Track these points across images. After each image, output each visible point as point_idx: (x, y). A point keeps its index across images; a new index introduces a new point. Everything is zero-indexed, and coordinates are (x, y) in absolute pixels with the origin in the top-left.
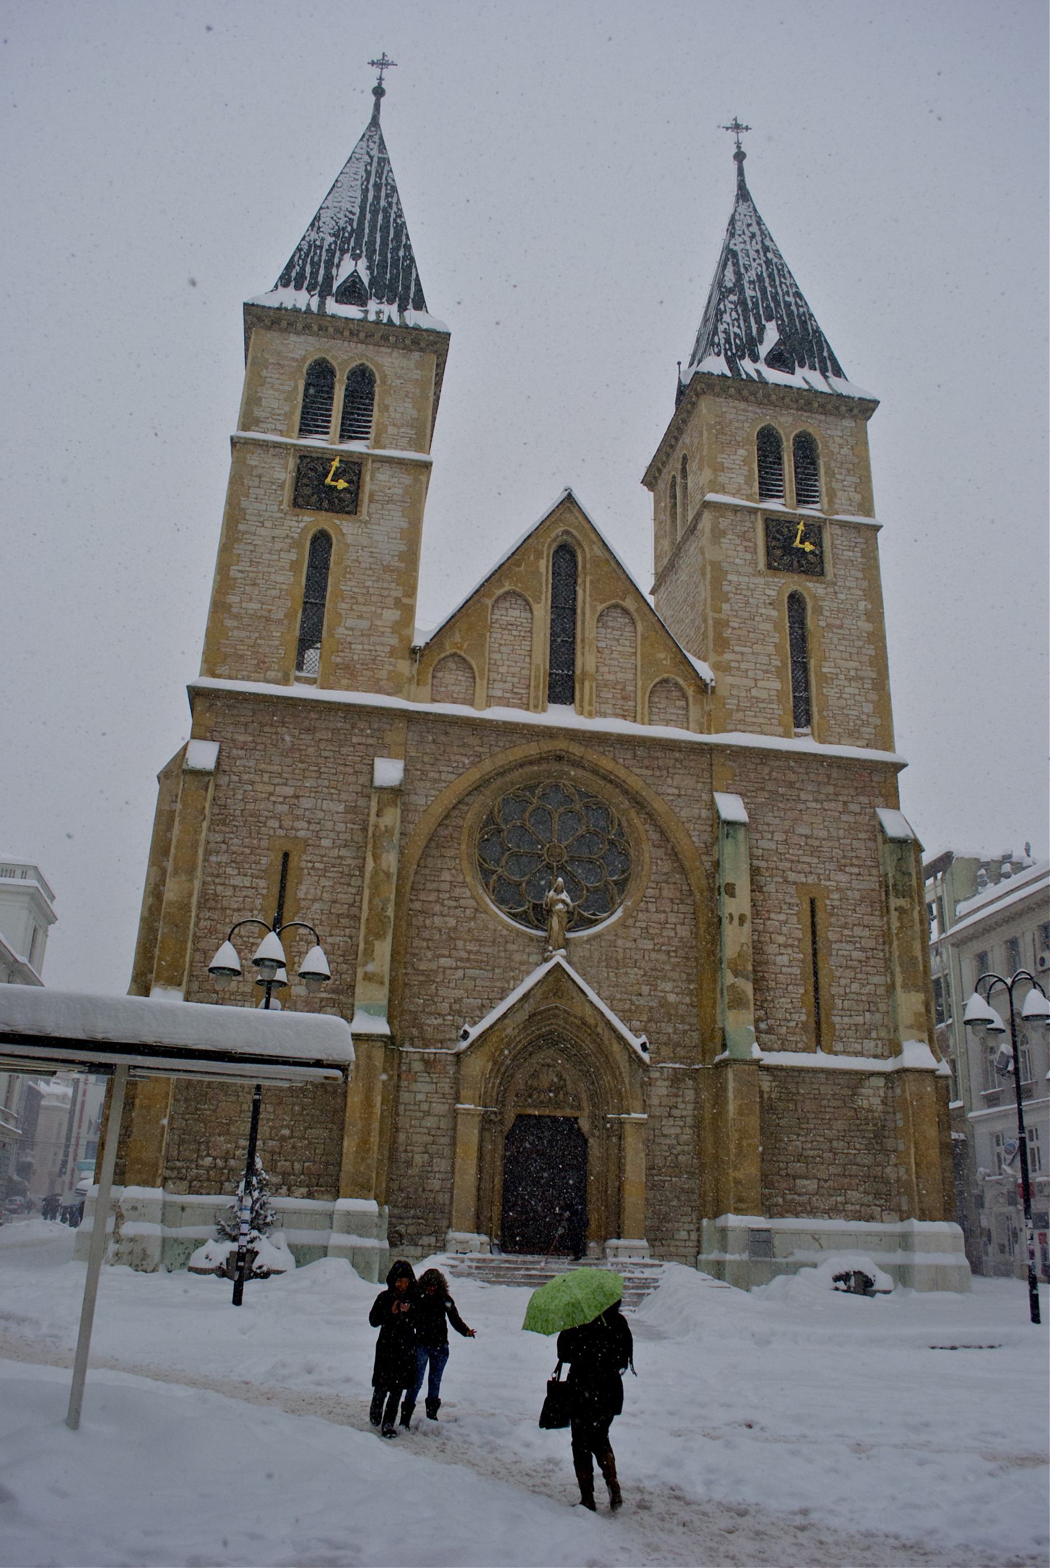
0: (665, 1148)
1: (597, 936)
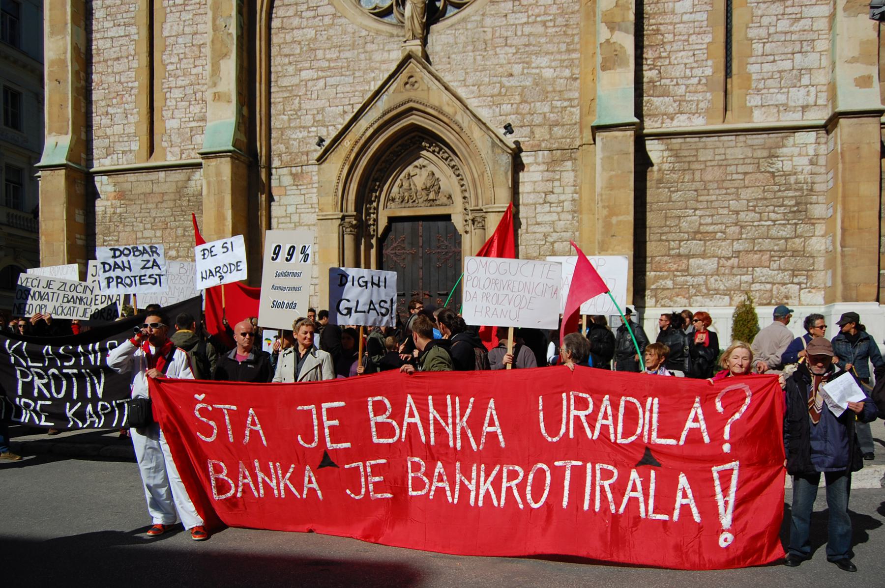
0: (541, 236)
1: (464, 20)
